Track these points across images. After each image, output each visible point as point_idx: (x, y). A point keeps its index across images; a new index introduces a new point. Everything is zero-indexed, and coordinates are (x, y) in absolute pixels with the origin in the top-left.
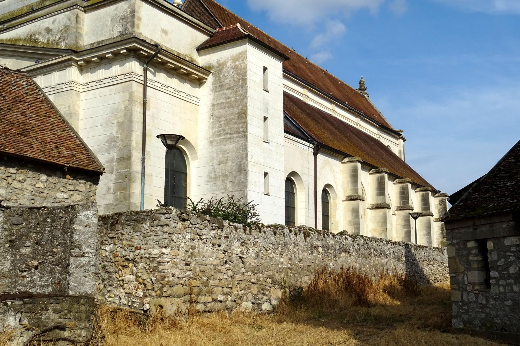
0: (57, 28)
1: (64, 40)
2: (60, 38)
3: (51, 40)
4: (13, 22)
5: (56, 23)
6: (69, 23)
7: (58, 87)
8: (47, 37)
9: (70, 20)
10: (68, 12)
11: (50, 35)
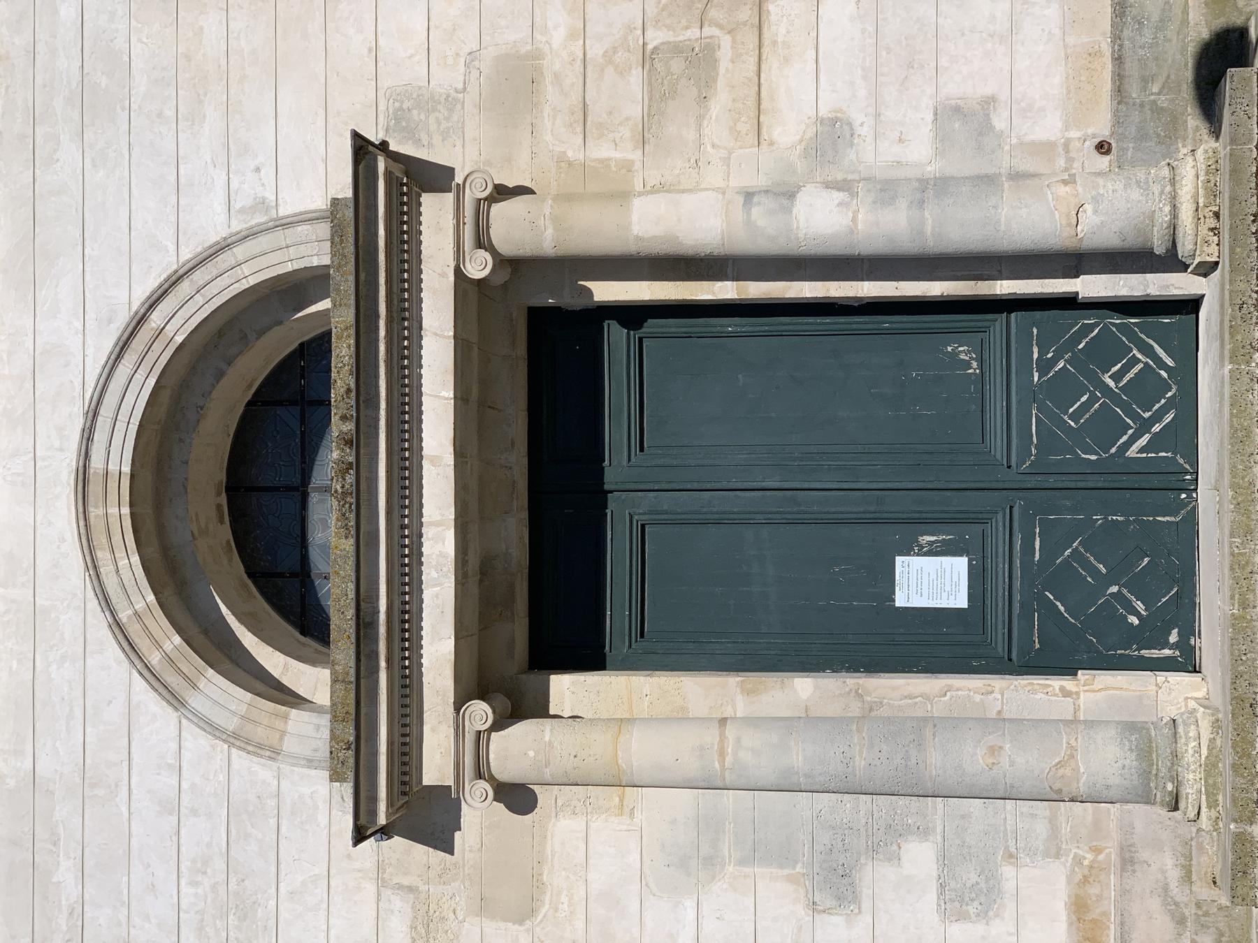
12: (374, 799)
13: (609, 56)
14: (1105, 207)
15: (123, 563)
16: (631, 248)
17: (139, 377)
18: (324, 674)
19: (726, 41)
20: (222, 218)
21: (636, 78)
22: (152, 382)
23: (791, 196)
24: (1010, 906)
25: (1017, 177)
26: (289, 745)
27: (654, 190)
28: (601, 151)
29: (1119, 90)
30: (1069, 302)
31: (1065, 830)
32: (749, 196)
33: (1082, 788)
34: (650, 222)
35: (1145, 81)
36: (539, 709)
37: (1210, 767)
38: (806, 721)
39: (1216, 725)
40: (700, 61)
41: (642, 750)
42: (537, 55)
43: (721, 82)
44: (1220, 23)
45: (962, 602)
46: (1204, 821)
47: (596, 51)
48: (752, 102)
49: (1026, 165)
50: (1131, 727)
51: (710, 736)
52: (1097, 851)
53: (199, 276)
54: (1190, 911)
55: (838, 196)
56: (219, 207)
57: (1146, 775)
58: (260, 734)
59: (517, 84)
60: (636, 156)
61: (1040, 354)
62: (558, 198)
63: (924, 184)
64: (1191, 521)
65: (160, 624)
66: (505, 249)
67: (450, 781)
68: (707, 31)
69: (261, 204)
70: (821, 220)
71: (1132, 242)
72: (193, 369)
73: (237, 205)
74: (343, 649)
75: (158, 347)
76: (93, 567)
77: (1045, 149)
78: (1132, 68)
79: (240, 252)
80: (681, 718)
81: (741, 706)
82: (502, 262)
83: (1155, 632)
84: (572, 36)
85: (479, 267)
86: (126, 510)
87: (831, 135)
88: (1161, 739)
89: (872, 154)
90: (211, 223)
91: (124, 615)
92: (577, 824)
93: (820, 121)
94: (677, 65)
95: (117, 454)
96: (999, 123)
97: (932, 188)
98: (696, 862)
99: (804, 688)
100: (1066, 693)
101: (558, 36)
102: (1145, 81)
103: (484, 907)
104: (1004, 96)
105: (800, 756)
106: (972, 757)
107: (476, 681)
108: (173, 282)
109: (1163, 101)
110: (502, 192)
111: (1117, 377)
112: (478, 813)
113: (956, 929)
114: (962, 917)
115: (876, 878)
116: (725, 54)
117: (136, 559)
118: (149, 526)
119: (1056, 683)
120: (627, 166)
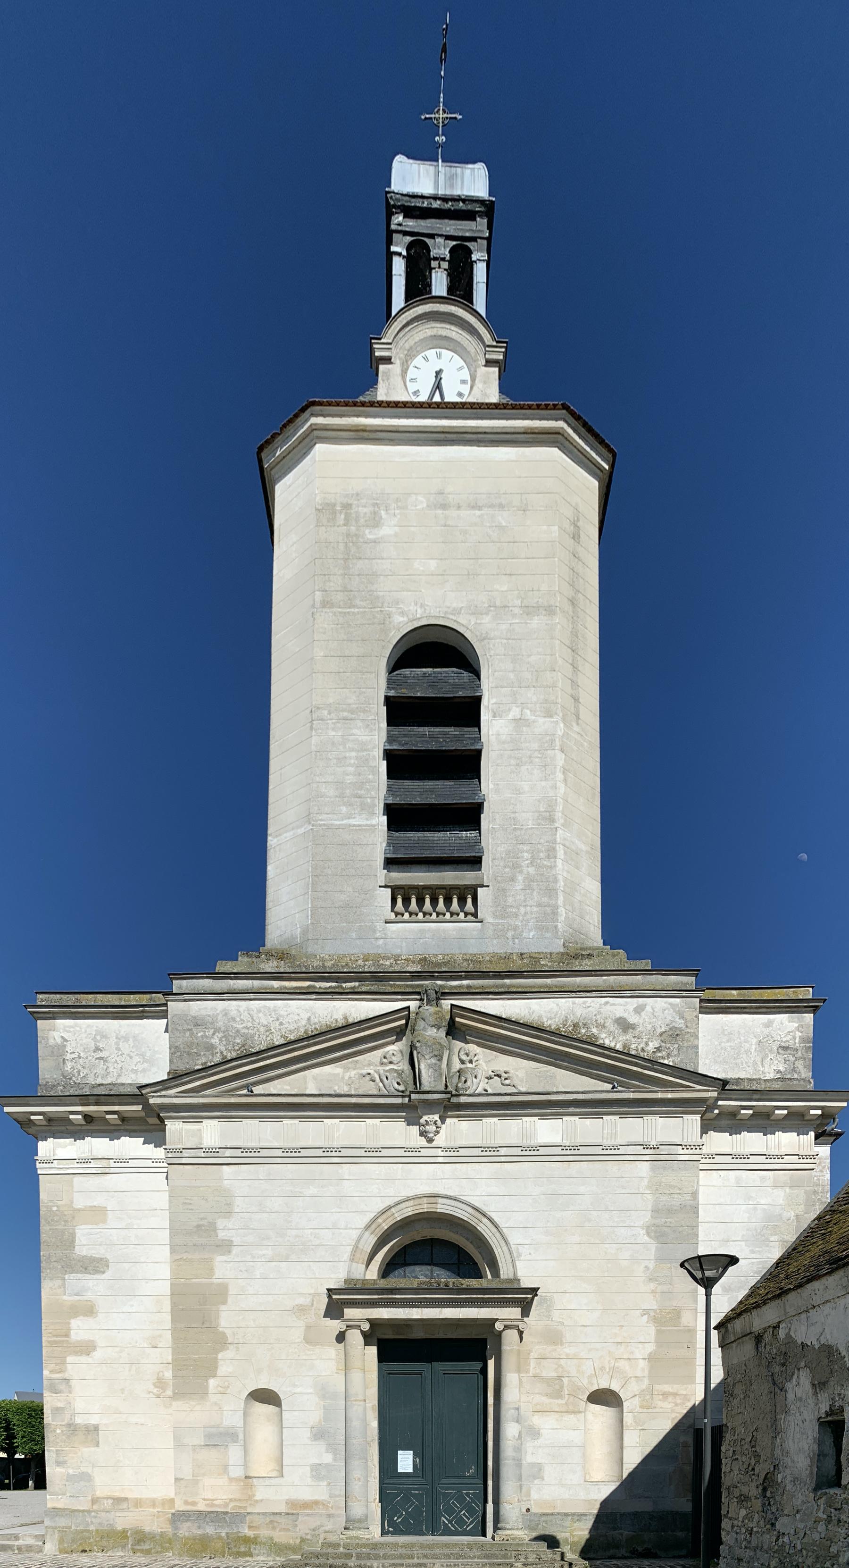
0: (649, 1027)
1: (669, 1056)
2: (658, 1049)
3: (633, 1046)
4: (507, 981)
5: (643, 1014)
6: (680, 1023)
7: (664, 1149)
8: (623, 1038)
9: (682, 1017)
10: (678, 1001)
11: (629, 1036)
12: (340, 1294)
13: (560, 1366)
14: (511, 1510)
15: (409, 1209)
16: (503, 1373)
17: (467, 1215)
18: (375, 1276)
19: (563, 1402)
20: (516, 1242)
21: (554, 1374)
22: (465, 1219)
23: (517, 1422)
24: (313, 1483)
25: (521, 1486)
26: (354, 1265)
27: (520, 1380)
28: (533, 1364)
29: (544, 1514)
30: (486, 1501)
31: (337, 1499)
32: (518, 1409)
33: (349, 1504)
34: (510, 1379)
35: (546, 1522)
36: (367, 1344)
37: (357, 1538)
38: (365, 1425)
39: (368, 1539)
40: (558, 1394)
41: (356, 1377)
42: (562, 1344)
43: (552, 1400)
44: (561, 1541)
45: (399, 1471)
46: (342, 1536)
47: (562, 1362)
48: (545, 1409)
49: (524, 1490)
50: (367, 1517)
51: (361, 1397)
52: (332, 1508)
53: (498, 1235)
54: (317, 1532)
55: (517, 1436)
56: (519, 1241)
57: (354, 1521)
58: (358, 1255)
59: (554, 1337)
60: (531, 1375)
61: (470, 1493)
62: (519, 1351)
63: (521, 1460)
64: (423, 1534)
65: (390, 1222)
66: (504, 1334)
67: (345, 1317)
68: (567, 1396)
69: (519, 1255)
70: (510, 1430)
71: (501, 1518)
72: (470, 1230)
73: (519, 1247)
74: (383, 1283)
75: (476, 1221)
76: (408, 1200)
77: (528, 1494)
78: (550, 1518)
79: (505, 1248)
80: (366, 1387)
81: (369, 1405)
82: (500, 1333)
83: (392, 1523)
84: (567, 1355)
85: (499, 1326)
86: (426, 1210)
87: (535, 1433)
88: (364, 1525)
89: (529, 1445)
90: (514, 1238)
91: (393, 1210)
92: (333, 1356)
93: (539, 1430)
94: (557, 1387)
95: (443, 1207)
96: (536, 1482)
97: (519, 1464)
98: (324, 1392)
99: (375, 1424)
100: (375, 1500)
101: (567, 1350)
102: (546, 1522)
103: (308, 1328)
104: (544, 1483)
105: (355, 1424)
106: (357, 1474)
107: (375, 1324)
108: (496, 1226)
109: (540, 1526)
110: (521, 1333)
111: (464, 1514)
112: (336, 1325)
113: (308, 1468)
114: (312, 1470)
115: (321, 1445)
116: (560, 1401)
117: (411, 1214)
118: (421, 1217)
119: (378, 1497)
120: (527, 1372)
